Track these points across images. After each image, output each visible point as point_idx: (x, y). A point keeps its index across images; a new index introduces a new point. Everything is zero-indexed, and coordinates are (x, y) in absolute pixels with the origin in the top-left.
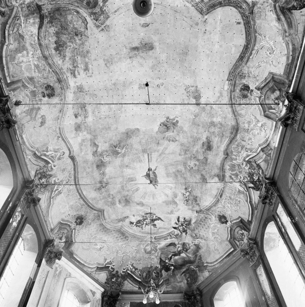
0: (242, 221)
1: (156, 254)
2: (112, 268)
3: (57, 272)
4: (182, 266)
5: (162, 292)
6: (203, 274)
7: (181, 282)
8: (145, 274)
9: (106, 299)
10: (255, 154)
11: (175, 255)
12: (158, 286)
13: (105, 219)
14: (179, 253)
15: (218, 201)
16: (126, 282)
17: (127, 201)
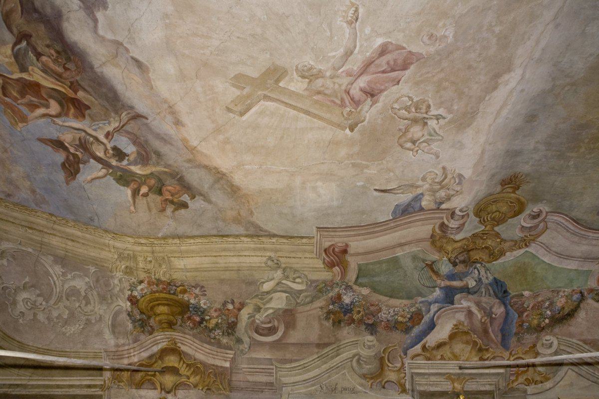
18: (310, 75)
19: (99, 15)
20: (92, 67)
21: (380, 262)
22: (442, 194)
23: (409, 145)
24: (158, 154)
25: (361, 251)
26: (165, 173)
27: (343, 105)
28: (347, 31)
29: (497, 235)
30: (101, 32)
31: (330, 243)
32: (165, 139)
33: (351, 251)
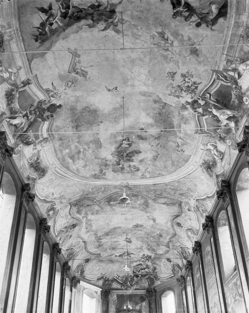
0: (178, 265)
1: (131, 269)
2: (105, 277)
3: (79, 289)
4: (145, 275)
5: (134, 289)
6: (157, 282)
7: (145, 283)
8: (124, 279)
9: (103, 294)
10: (184, 247)
11: (142, 269)
12: (132, 285)
13: (101, 257)
14: (144, 269)
15: (166, 253)
16: (113, 283)
17: (114, 249)
18: (79, 62)
19: (87, 26)
20: (76, 22)
21: (28, 93)
22: (55, 95)
23: (67, 83)
24: (53, 34)
25: (31, 87)
26: (48, 36)
27: (74, 69)
28: (89, 66)
29: (44, 113)
30: (84, 26)
31: (31, 79)
32: (58, 36)
33: (30, 85)
